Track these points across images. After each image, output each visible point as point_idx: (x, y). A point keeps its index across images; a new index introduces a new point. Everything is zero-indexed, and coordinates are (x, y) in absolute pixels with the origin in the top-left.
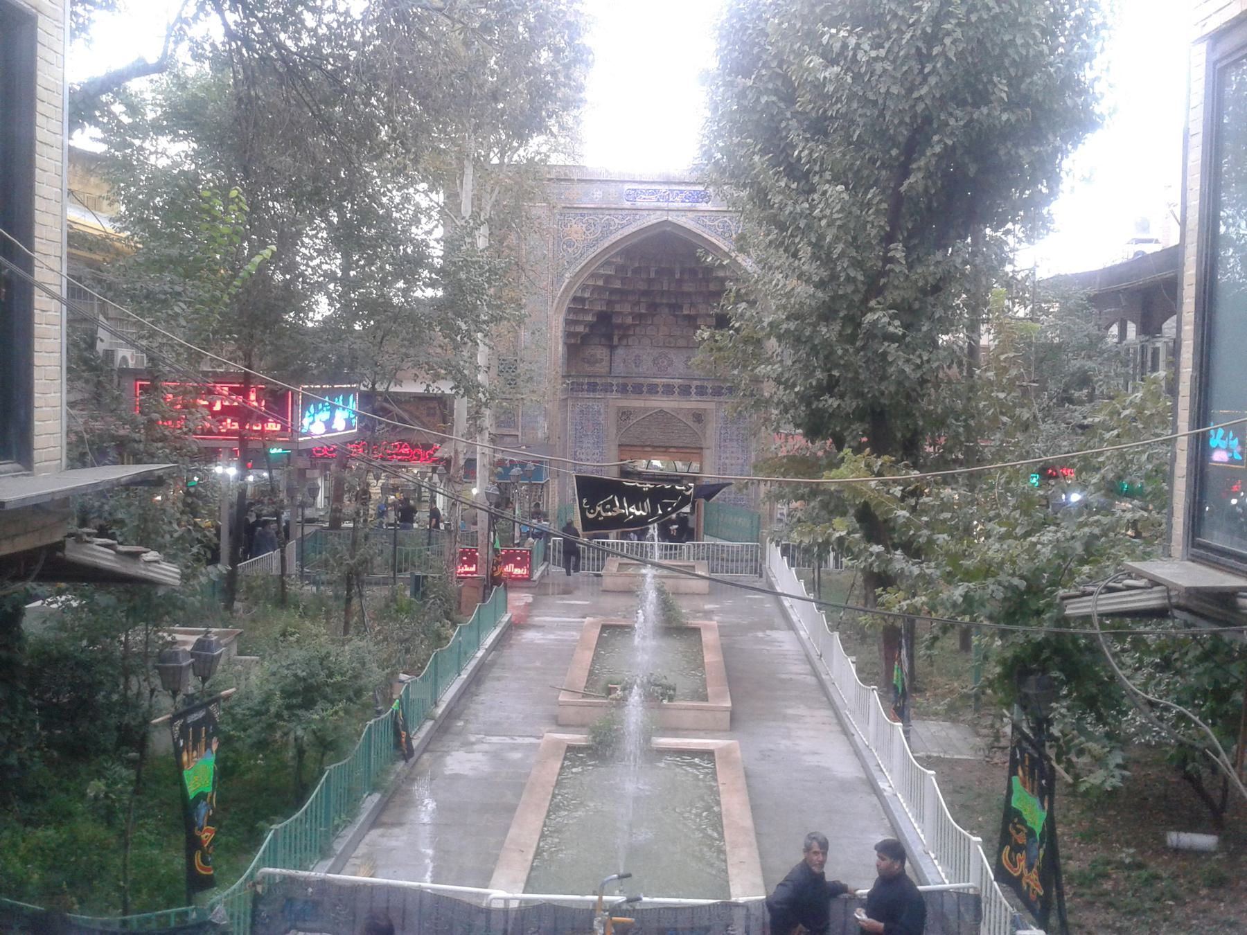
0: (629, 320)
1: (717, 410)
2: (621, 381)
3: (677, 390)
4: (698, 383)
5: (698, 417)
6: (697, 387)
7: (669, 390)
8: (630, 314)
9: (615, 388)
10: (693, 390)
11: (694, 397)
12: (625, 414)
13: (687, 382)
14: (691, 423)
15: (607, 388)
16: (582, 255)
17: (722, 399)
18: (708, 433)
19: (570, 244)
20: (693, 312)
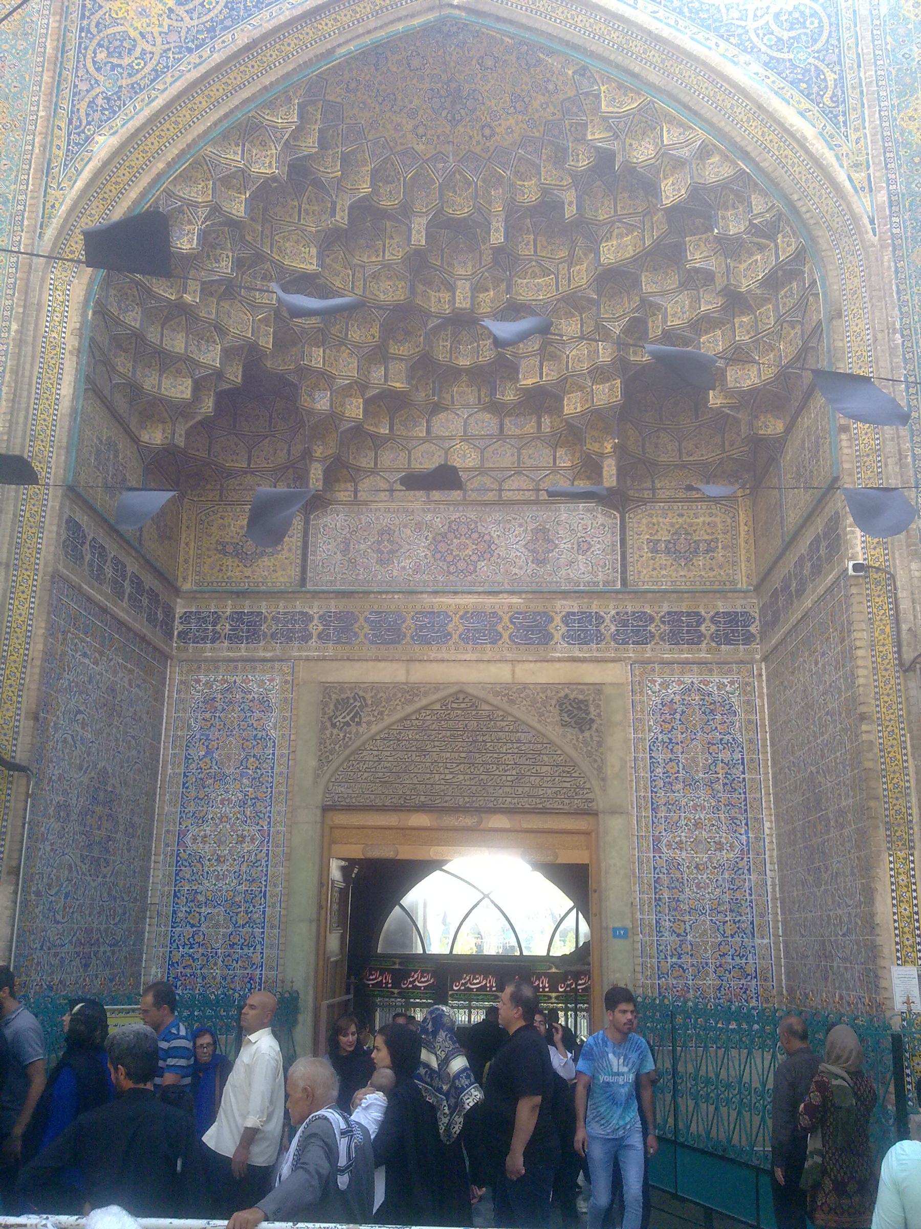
0: (354, 409)
1: (637, 687)
2: (334, 606)
3: (506, 630)
4: (572, 605)
5: (579, 710)
6: (567, 618)
7: (482, 631)
8: (361, 386)
9: (315, 627)
10: (558, 629)
11: (562, 649)
12: (344, 707)
13: (537, 606)
14: (554, 732)
15: (293, 630)
16: (157, 74)
17: (649, 652)
18: (613, 761)
19: (119, 46)
20: (550, 374)
